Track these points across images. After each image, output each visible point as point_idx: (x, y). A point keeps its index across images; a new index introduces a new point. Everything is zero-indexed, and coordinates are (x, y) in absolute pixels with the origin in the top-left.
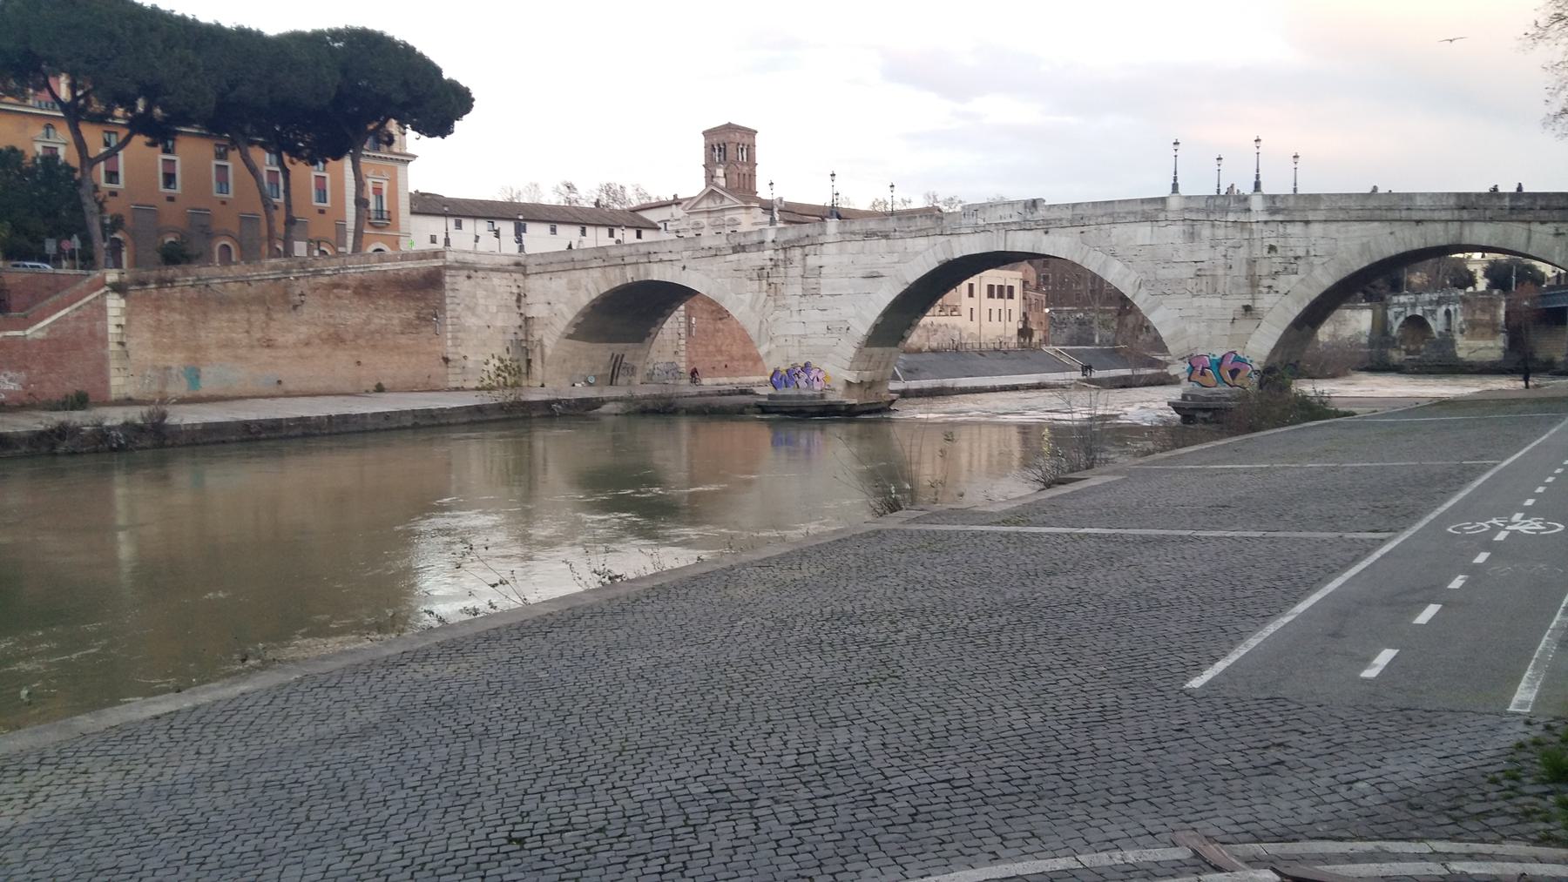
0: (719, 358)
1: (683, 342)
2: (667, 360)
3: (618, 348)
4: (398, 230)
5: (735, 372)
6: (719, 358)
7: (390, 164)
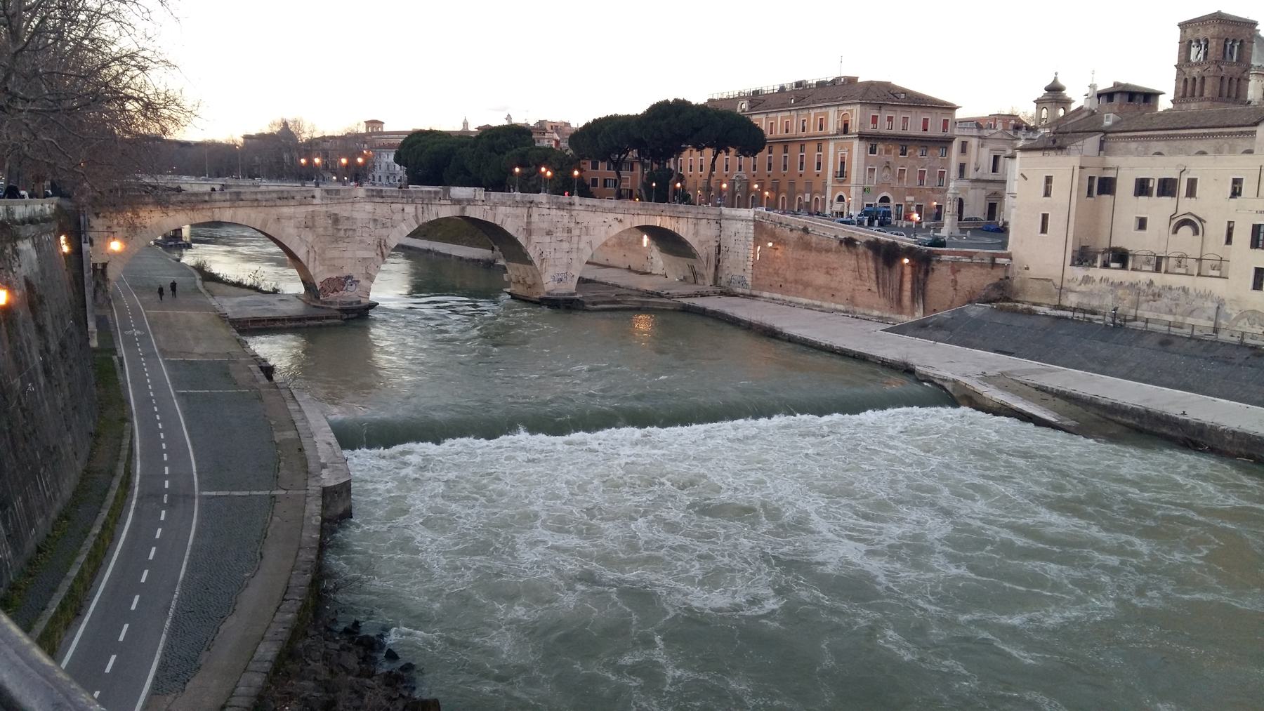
0: (776, 279)
1: (751, 264)
2: (739, 274)
3: (689, 260)
4: (850, 183)
5: (788, 292)
6: (776, 279)
7: (850, 141)
